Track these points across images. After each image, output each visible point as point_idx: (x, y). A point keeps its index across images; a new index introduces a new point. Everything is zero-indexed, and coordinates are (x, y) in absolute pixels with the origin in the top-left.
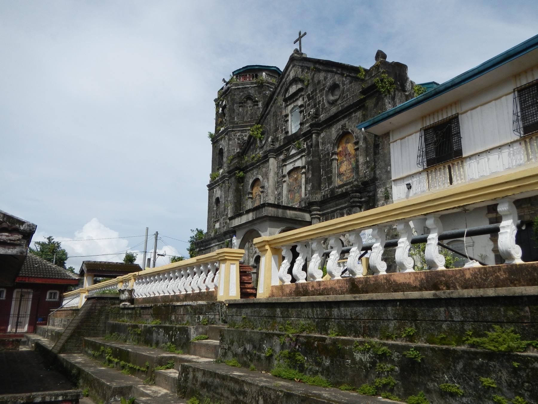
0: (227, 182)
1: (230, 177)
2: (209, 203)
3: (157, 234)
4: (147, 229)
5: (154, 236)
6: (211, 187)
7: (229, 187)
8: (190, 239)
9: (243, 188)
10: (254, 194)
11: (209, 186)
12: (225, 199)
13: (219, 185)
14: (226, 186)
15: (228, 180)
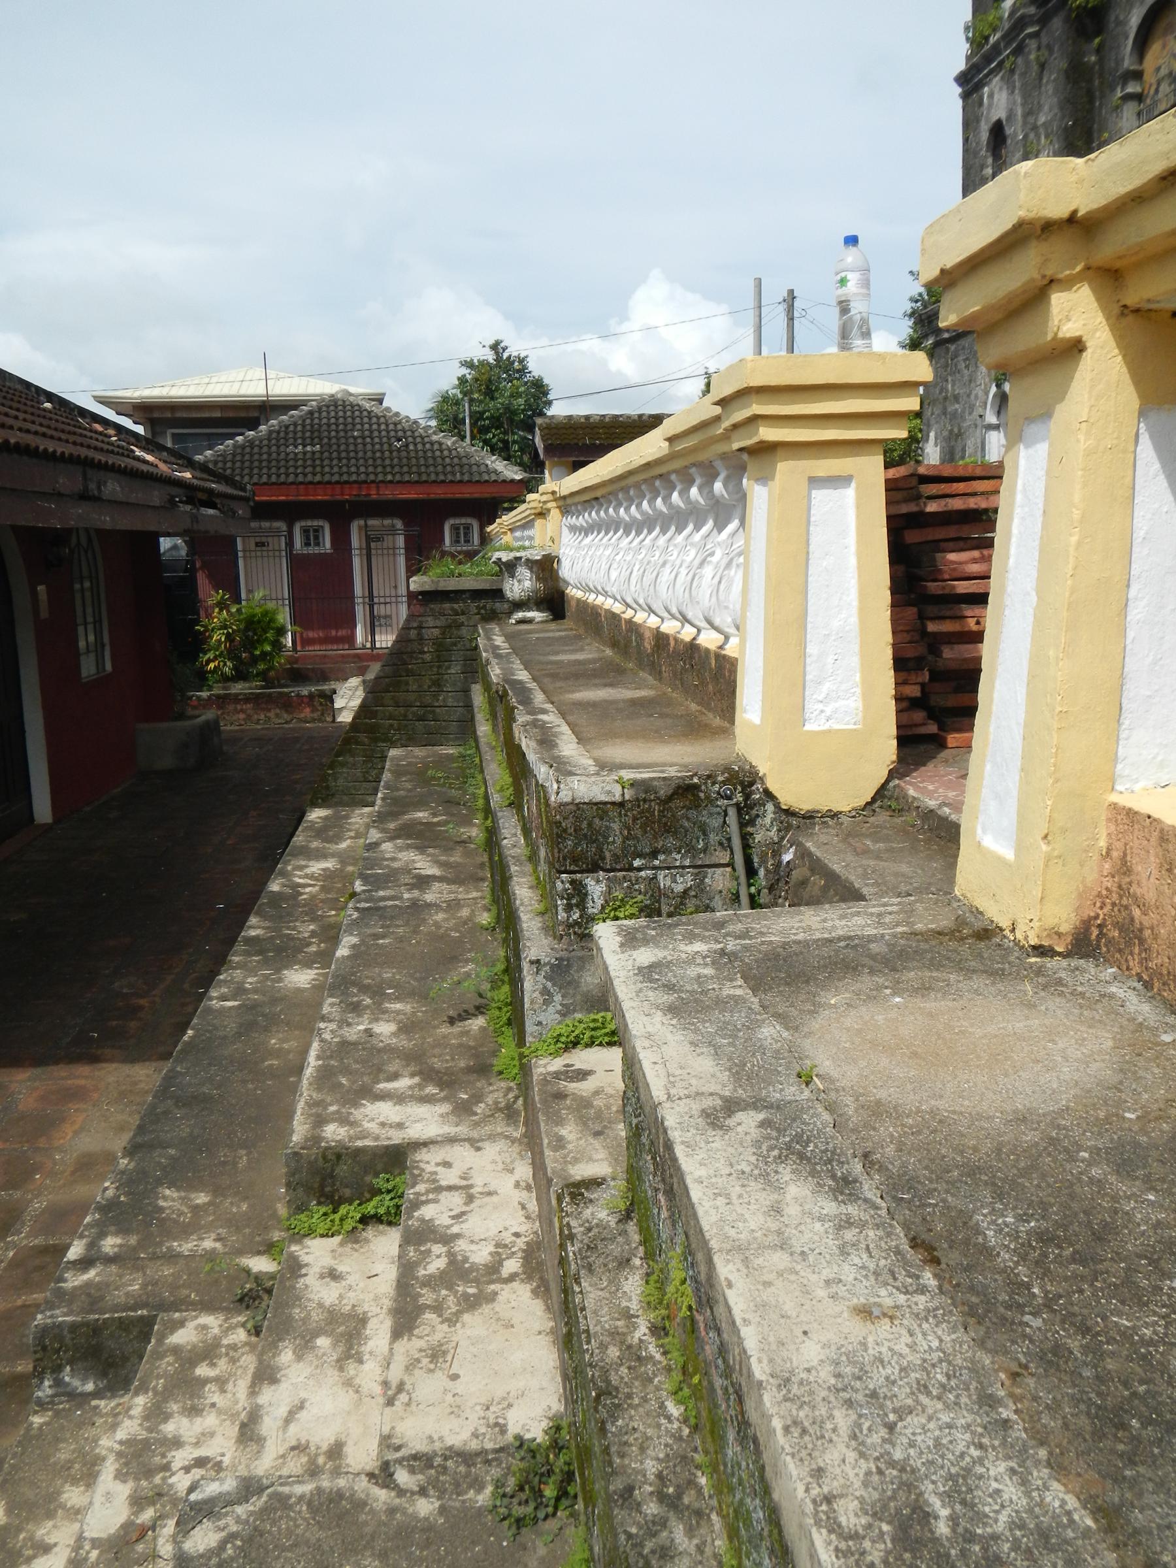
0: (1033, 44)
1: (1044, 21)
2: (966, 151)
3: (791, 298)
4: (759, 283)
5: (784, 306)
6: (971, 82)
7: (1042, 66)
8: (908, 306)
9: (1101, 61)
10: (1149, 77)
11: (963, 79)
12: (1025, 123)
13: (1000, 65)
14: (1027, 63)
15: (1036, 35)
